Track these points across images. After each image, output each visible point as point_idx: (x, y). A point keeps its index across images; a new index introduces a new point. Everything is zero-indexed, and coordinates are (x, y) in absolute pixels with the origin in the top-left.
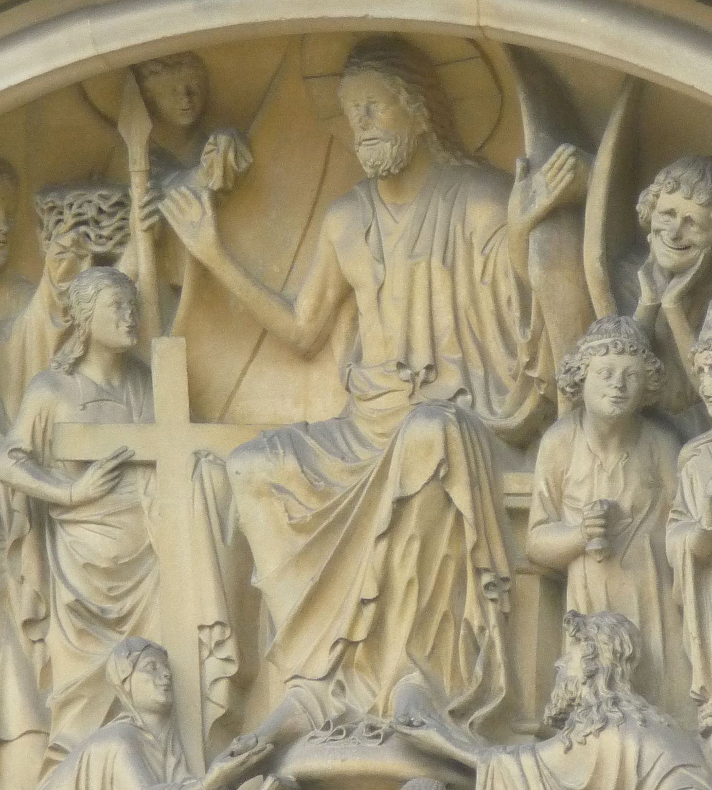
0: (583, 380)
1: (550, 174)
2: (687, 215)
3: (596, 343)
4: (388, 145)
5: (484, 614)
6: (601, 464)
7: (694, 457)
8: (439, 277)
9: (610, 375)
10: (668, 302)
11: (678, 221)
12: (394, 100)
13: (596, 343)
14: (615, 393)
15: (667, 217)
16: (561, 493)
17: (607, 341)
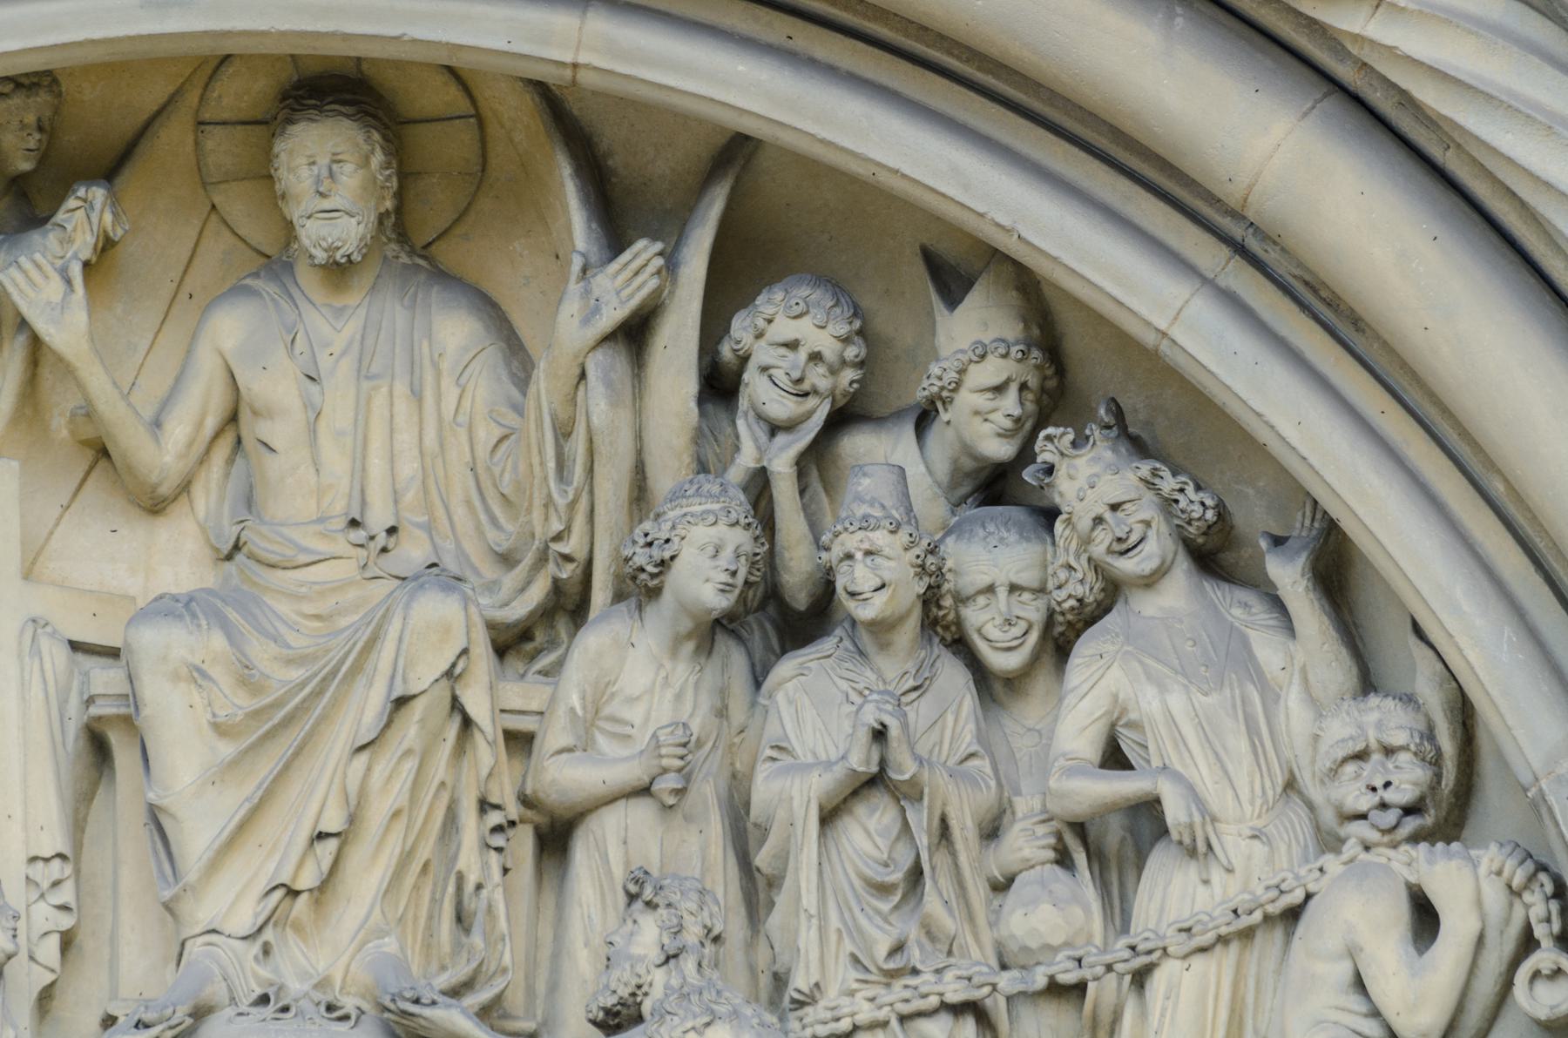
2: (816, 349)
6: (667, 677)
7: (801, 678)
11: (802, 355)
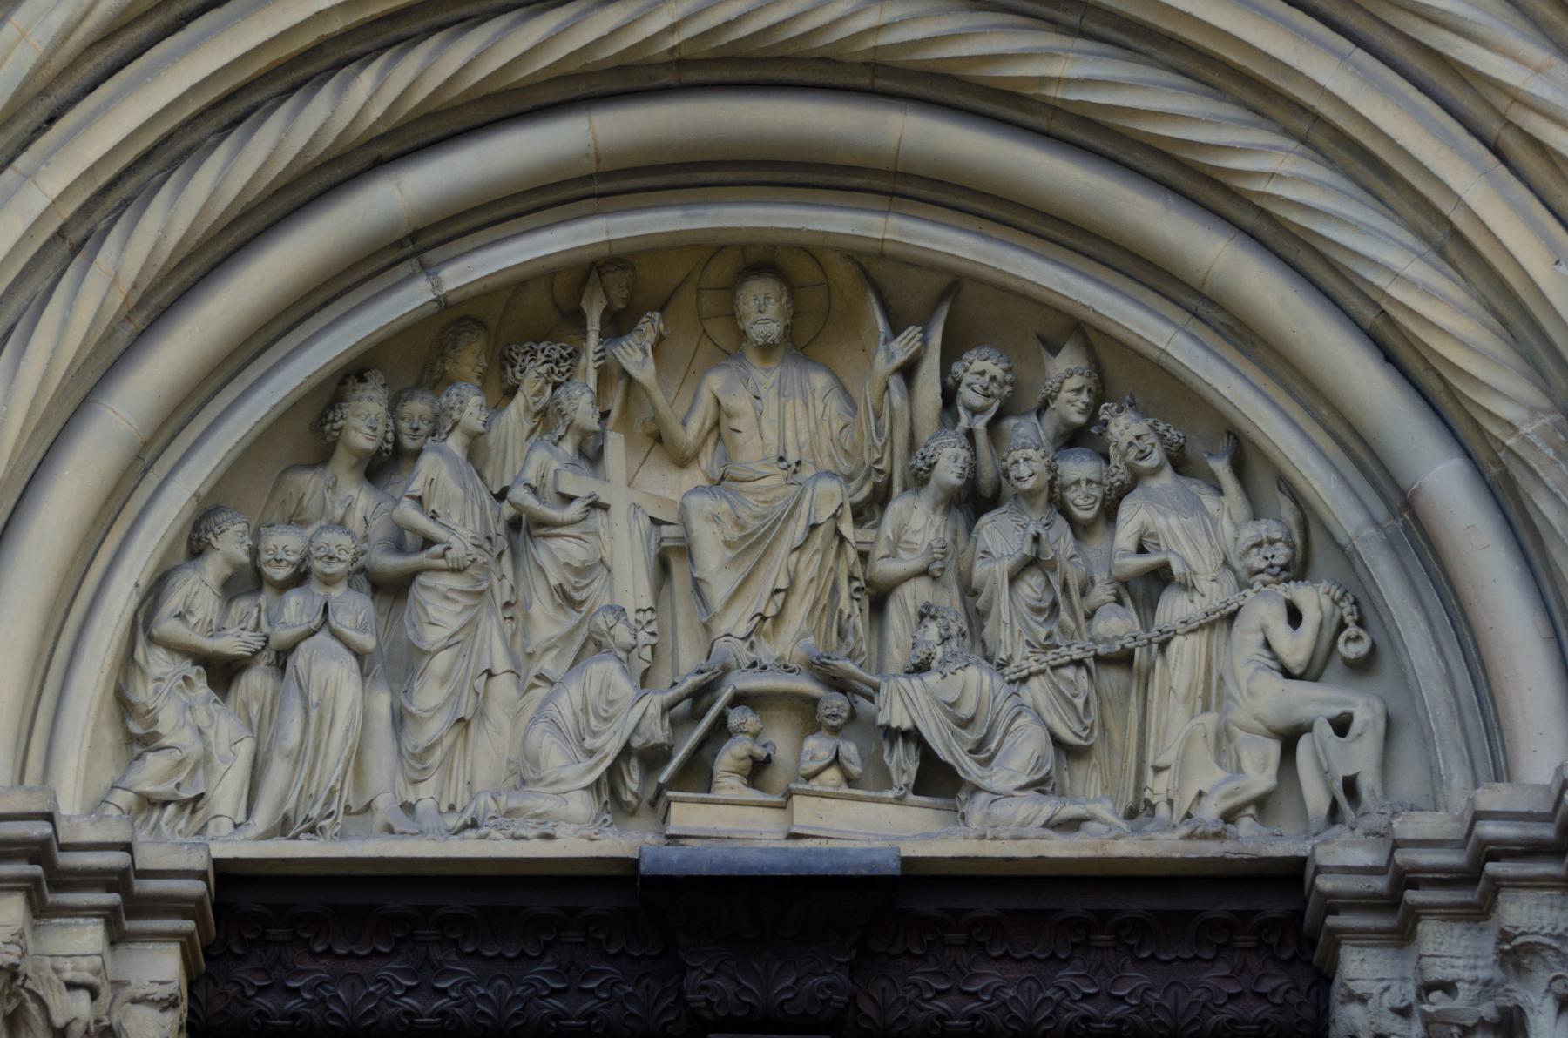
0: (936, 463)
3: (945, 441)
8: (800, 410)
9: (955, 461)
10: (980, 424)
14: (960, 471)
16: (899, 539)
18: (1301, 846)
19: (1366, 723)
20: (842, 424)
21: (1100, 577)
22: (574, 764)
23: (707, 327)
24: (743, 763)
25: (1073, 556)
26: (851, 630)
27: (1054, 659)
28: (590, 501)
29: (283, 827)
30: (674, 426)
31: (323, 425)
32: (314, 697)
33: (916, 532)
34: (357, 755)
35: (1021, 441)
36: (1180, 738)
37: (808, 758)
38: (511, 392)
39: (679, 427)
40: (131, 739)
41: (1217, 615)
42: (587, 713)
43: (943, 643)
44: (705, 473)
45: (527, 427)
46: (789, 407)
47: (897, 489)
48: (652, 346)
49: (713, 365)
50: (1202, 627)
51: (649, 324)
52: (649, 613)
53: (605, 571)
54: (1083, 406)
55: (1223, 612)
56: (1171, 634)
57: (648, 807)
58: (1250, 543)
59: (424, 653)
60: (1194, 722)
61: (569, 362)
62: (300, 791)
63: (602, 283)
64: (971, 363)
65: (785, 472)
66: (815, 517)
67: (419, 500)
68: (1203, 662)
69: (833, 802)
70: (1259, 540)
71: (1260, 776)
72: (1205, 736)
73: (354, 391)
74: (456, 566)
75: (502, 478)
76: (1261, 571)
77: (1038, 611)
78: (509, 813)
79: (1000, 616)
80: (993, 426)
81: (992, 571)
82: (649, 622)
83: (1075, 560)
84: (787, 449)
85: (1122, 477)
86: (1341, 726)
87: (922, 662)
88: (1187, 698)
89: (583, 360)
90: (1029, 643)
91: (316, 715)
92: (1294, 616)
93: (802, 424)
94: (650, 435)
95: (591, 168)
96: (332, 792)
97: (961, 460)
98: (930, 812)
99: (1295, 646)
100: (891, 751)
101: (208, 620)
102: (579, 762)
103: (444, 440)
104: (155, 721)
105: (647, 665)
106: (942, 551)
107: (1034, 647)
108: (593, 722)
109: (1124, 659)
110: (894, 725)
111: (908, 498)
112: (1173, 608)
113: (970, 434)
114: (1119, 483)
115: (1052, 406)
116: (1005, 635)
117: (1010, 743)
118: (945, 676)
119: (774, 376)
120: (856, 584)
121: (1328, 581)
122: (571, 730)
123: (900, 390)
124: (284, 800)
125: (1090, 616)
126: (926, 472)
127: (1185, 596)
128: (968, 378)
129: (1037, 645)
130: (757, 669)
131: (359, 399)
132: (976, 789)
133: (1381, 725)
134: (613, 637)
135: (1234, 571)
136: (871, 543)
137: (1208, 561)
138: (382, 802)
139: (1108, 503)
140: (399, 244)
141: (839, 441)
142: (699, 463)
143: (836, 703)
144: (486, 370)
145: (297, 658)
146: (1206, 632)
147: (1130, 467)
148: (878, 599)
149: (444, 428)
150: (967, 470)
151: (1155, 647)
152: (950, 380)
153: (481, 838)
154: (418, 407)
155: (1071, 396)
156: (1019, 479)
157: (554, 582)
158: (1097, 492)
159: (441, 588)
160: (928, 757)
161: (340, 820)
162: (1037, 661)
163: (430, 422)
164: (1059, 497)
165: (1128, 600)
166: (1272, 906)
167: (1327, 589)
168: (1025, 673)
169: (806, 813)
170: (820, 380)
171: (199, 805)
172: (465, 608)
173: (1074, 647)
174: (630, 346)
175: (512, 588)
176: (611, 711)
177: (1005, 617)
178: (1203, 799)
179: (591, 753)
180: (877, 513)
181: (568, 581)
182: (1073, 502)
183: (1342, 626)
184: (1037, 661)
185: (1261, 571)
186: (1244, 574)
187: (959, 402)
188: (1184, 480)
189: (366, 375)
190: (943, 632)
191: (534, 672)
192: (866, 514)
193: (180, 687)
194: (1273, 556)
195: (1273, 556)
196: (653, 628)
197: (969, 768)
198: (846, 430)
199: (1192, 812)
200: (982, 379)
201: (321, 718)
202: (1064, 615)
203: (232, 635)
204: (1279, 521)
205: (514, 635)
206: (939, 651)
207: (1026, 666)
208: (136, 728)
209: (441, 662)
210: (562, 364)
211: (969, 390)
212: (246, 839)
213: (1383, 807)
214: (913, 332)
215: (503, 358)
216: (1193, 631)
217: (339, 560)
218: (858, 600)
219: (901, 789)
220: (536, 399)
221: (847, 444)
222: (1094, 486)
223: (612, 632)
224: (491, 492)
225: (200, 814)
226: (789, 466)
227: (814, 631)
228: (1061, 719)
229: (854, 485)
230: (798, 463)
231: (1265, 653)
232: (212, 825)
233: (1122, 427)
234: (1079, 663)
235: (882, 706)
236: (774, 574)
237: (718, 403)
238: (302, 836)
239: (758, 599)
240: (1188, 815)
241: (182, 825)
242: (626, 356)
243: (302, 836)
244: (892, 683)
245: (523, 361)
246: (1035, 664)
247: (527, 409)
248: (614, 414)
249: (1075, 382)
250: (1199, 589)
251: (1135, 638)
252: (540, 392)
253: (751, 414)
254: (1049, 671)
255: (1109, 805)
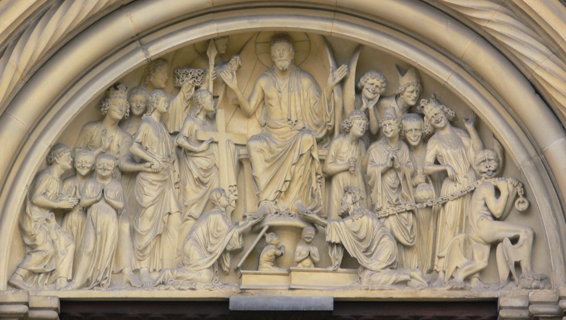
0: (352, 126)
1: (339, 72)
3: (356, 117)
4: (287, 62)
5: (317, 185)
8: (297, 97)
9: (360, 126)
10: (371, 107)
11: (374, 86)
12: (289, 50)
13: (356, 117)
15: (371, 85)
16: (337, 155)
17: (360, 116)
18: (496, 293)
19: (524, 240)
20: (315, 101)
21: (419, 171)
22: (204, 258)
23: (259, 57)
24: (271, 258)
25: (409, 162)
26: (316, 195)
27: (399, 210)
28: (210, 142)
29: (87, 284)
30: (245, 104)
31: (101, 108)
32: (99, 230)
33: (344, 153)
34: (116, 250)
35: (388, 116)
36: (449, 245)
37: (298, 254)
38: (179, 88)
39: (247, 103)
40: (25, 245)
41: (466, 192)
42: (209, 235)
43: (354, 203)
44: (258, 121)
45: (184, 106)
46: (293, 96)
47: (337, 133)
48: (236, 71)
49: (263, 75)
50: (459, 197)
51: (235, 62)
52: (234, 187)
53: (216, 169)
54: (414, 98)
55: (468, 191)
56: (447, 200)
57: (233, 271)
58: (480, 161)
59: (142, 207)
60: (456, 237)
61: (201, 77)
62: (94, 269)
63: (215, 43)
64: (368, 79)
65: (291, 126)
66: (302, 151)
67: (141, 143)
68: (460, 211)
69: (307, 273)
70: (484, 159)
71: (481, 263)
72: (459, 244)
73: (113, 94)
74: (156, 171)
75: (174, 128)
76: (485, 173)
77: (393, 189)
78: (177, 278)
79: (377, 190)
80: (377, 106)
81: (375, 171)
82: (234, 191)
83: (409, 163)
84: (292, 115)
85: (429, 130)
86: (514, 240)
87: (345, 212)
88: (452, 228)
89: (207, 76)
90: (389, 202)
91: (99, 236)
92: (497, 192)
93: (298, 103)
94: (235, 105)
95: (211, 6)
96: (106, 269)
97: (362, 125)
98: (347, 275)
99: (497, 207)
100: (332, 250)
101: (55, 192)
102: (206, 257)
103: (150, 115)
104: (35, 240)
105: (233, 209)
106: (354, 163)
107: (391, 204)
108: (211, 239)
109: (429, 208)
110: (333, 241)
111: (341, 139)
112: (449, 188)
113: (367, 111)
114: (428, 133)
115: (401, 97)
116: (379, 198)
117: (380, 248)
118: (354, 221)
119: (287, 82)
120: (319, 177)
121: (512, 178)
122: (203, 244)
123: (338, 93)
124: (87, 271)
125: (415, 187)
126: (348, 130)
127: (453, 184)
128: (367, 86)
129: (392, 204)
130: (278, 215)
131: (116, 97)
132: (365, 268)
133: (531, 240)
134: (219, 202)
135: (474, 171)
136: (326, 156)
137: (463, 170)
138: (127, 271)
139: (424, 137)
140: (133, 37)
141: (313, 108)
142: (256, 117)
143: (309, 232)
144: (167, 80)
145: (91, 213)
146: (461, 199)
147: (432, 125)
148: (329, 178)
149: (151, 110)
150: (365, 129)
151: (440, 205)
152: (359, 85)
153: (167, 289)
154: (139, 97)
155: (409, 94)
156: (386, 132)
157: (195, 177)
158: (419, 134)
159: (149, 180)
160: (346, 253)
161: (110, 281)
162: (392, 210)
163: (144, 103)
164: (404, 135)
165: (430, 181)
166: (485, 314)
167: (511, 182)
168: (387, 215)
169: (297, 279)
170: (306, 82)
171: (53, 272)
172: (159, 187)
173: (407, 205)
174: (227, 72)
175: (179, 175)
176: (219, 234)
177: (380, 191)
178: (458, 270)
179: (211, 253)
180: (329, 140)
181: (201, 175)
182: (409, 138)
183: (517, 196)
184: (392, 210)
185: (485, 173)
186: (478, 172)
187: (363, 95)
188: (455, 130)
189: (118, 87)
190: (353, 200)
191: (187, 214)
192: (324, 140)
193: (45, 224)
194: (490, 167)
195: (490, 167)
196: (236, 193)
197: (363, 259)
198: (316, 104)
199: (453, 275)
200: (372, 86)
201: (102, 237)
202: (403, 191)
203: (65, 200)
204: (493, 150)
205: (179, 195)
206: (352, 207)
207: (387, 212)
208: (28, 241)
209: (149, 211)
210: (199, 78)
211: (367, 91)
212: (72, 289)
213: (530, 277)
214: (344, 67)
215: (174, 74)
216: (456, 199)
217: (108, 170)
218: (320, 183)
219: (335, 267)
220: (188, 94)
221: (317, 110)
222: (418, 131)
223: (219, 200)
224: (170, 134)
225: (54, 275)
226: (292, 123)
227: (301, 197)
228: (401, 234)
229: (319, 130)
230: (296, 121)
231: (485, 209)
232: (58, 280)
233: (429, 109)
234: (409, 211)
235: (328, 234)
236: (285, 174)
237: (263, 91)
238: (95, 288)
239: (278, 185)
240: (452, 277)
241: (46, 281)
242: (225, 76)
243: (95, 288)
244: (332, 223)
245: (183, 76)
246: (391, 211)
247: (184, 98)
248: (220, 98)
249: (410, 89)
250: (459, 181)
251: (432, 202)
252: (190, 91)
253: (277, 99)
254: (397, 214)
255: (420, 273)
